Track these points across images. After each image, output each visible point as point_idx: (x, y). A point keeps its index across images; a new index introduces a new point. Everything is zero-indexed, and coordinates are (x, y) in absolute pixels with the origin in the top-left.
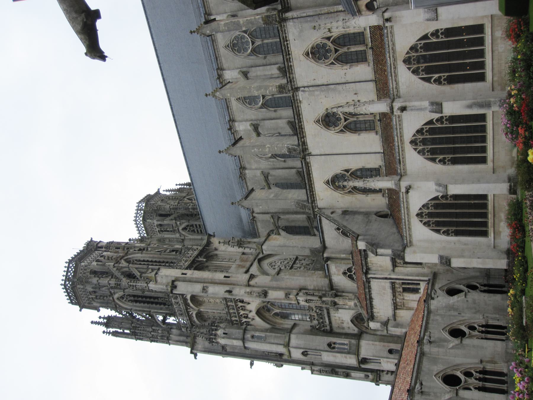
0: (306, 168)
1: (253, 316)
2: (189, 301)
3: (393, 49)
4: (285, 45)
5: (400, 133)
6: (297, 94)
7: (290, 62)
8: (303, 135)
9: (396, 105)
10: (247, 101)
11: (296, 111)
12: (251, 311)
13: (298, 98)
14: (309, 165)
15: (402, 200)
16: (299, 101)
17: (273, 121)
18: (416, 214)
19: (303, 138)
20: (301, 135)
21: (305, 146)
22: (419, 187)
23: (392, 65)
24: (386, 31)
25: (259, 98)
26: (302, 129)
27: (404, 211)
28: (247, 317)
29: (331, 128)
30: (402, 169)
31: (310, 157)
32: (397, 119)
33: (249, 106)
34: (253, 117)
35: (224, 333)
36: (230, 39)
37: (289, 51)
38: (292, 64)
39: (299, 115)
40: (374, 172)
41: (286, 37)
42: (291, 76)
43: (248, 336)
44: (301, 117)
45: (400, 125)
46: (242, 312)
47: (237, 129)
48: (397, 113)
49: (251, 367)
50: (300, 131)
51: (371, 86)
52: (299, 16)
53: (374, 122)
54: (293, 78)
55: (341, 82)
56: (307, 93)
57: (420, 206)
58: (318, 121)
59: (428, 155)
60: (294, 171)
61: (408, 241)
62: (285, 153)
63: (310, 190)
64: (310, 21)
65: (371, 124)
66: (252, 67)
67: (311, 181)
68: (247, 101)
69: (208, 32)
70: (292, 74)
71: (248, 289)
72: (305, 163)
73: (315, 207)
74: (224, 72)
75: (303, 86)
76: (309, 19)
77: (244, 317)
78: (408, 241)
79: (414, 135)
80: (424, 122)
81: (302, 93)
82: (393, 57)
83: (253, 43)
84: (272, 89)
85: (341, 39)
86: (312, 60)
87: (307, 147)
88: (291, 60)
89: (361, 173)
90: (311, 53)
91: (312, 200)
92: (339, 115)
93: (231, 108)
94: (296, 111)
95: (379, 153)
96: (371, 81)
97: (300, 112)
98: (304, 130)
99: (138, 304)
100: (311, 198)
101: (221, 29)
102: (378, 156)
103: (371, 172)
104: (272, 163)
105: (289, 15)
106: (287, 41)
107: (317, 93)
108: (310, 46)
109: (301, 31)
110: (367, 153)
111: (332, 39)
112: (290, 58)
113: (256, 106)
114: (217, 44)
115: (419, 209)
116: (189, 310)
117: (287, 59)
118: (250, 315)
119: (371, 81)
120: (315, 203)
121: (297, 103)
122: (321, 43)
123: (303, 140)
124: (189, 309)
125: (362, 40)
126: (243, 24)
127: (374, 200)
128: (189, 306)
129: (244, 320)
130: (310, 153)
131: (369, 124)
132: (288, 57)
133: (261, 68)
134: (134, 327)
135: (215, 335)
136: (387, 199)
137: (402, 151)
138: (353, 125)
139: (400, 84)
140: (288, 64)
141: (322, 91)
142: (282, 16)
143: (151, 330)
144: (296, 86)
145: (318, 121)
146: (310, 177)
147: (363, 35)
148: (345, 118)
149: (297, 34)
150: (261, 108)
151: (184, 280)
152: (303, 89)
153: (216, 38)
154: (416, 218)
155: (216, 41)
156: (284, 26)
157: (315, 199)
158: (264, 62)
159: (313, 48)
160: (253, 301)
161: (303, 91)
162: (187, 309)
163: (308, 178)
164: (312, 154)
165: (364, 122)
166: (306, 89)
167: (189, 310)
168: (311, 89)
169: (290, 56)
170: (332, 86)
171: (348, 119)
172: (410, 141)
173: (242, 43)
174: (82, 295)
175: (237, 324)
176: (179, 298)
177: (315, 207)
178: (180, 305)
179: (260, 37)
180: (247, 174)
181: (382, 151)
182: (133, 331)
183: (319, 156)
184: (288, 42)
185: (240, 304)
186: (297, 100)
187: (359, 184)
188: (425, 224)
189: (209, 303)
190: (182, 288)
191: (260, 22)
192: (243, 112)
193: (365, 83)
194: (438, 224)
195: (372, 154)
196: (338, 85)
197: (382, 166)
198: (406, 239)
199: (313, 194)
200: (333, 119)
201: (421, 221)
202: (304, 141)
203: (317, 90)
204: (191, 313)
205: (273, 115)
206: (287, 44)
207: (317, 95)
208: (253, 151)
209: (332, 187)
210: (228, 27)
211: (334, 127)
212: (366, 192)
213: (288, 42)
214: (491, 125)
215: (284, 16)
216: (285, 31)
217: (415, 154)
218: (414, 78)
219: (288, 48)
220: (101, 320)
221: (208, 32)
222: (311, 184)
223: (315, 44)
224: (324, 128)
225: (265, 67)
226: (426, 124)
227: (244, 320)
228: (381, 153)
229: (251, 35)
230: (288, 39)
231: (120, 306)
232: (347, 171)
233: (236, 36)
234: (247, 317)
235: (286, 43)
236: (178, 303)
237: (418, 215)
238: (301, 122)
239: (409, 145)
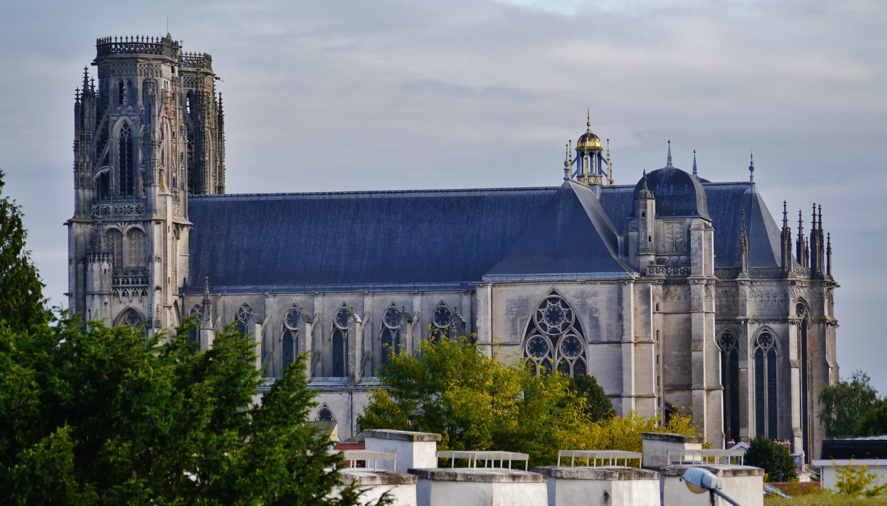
1: (125, 303)
2: (133, 225)
10: (341, 313)
12: (131, 301)
17: (321, 337)
28: (124, 295)
33: (336, 314)
34: (325, 316)
35: (105, 270)
43: (107, 299)
46: (130, 292)
47: (316, 299)
49: (64, 294)
56: (347, 400)
60: (271, 349)
66: (372, 326)
68: (341, 313)
71: (160, 308)
74: (371, 297)
77: (124, 293)
83: (393, 330)
99: (119, 146)
101: (402, 334)
104: (278, 326)
113: (335, 321)
116: (123, 223)
118: (125, 299)
124: (125, 224)
128: (128, 224)
129: (120, 292)
133: (370, 335)
134: (90, 136)
135: (103, 260)
141: (348, 412)
143: (88, 160)
150: (334, 326)
151: (165, 232)
158: (376, 338)
160: (144, 306)
161: (349, 398)
162: (125, 222)
166: (350, 400)
167: (123, 223)
173: (395, 319)
174: (125, 65)
175: (114, 283)
176: (139, 215)
178: (129, 213)
180: (268, 299)
182: (85, 137)
185: (140, 292)
189: (129, 245)
190: (157, 230)
192: (331, 307)
203: (348, 408)
204: (119, 224)
205: (327, 337)
220: (90, 84)
225: (370, 340)
227: (120, 292)
231: (115, 121)
234: (124, 295)
236: (131, 212)
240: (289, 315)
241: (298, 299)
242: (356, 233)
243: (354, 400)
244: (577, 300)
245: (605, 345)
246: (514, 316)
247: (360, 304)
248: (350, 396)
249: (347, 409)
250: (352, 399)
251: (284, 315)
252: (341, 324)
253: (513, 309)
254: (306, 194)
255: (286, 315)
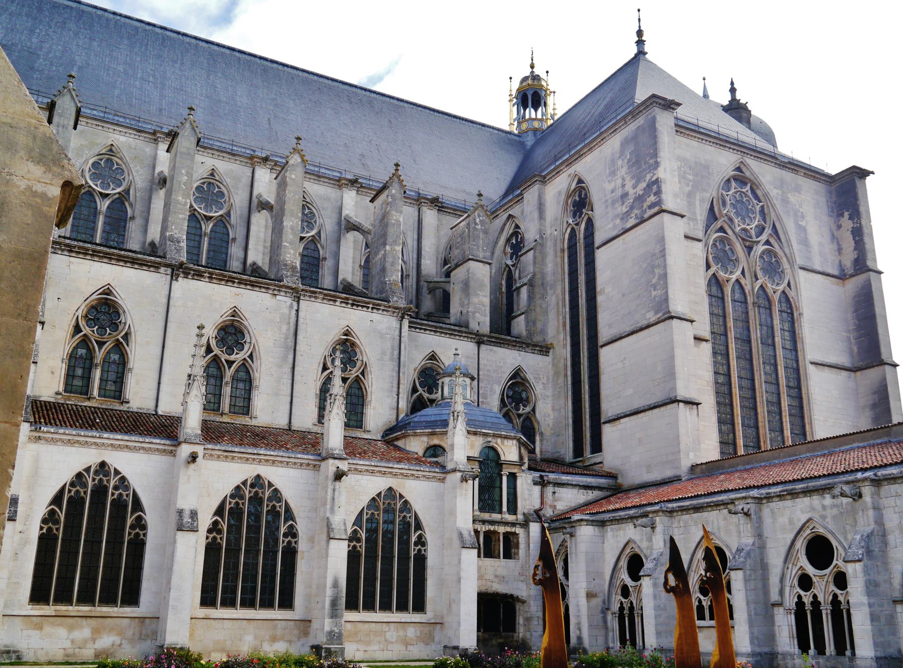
0: (148, 262)
3: (413, 475)
4: (369, 303)
5: (282, 462)
6: (288, 295)
7: (341, 302)
8: (215, 278)
9: (344, 465)
10: (205, 186)
11: (262, 283)
13: (282, 294)
14: (152, 269)
15: (147, 440)
16: (276, 292)
18: (108, 461)
19: (209, 277)
20: (216, 275)
21: (194, 275)
22: (189, 478)
23: (390, 470)
24: (437, 470)
25: (206, 208)
26: (228, 281)
27: (122, 440)
29: (216, 331)
30: (213, 452)
31: (169, 277)
32: (306, 462)
36: (315, 205)
37: (358, 306)
38: (338, 303)
39: (253, 286)
40: (113, 388)
41: (378, 309)
42: (321, 296)
44: (248, 287)
45: (295, 463)
48: (332, 465)
50: (225, 276)
51: (281, 421)
52: (402, 339)
53: (214, 410)
54: (316, 297)
55: (296, 373)
56: (287, 311)
57: (125, 472)
58: (234, 314)
59: (230, 503)
61: (41, 435)
62: (169, 229)
63: (99, 252)
64: (392, 354)
65: (212, 405)
67: (119, 260)
68: (205, 186)
69: (394, 191)
70: (323, 299)
72: (160, 264)
73: (55, 249)
75: (300, 309)
76: (396, 353)
78: (41, 435)
79: (270, 485)
80: (292, 505)
81: (288, 304)
82: (402, 474)
84: (290, 254)
85: (357, 392)
86: (337, 338)
87: (190, 277)
88: (344, 305)
89: (114, 362)
90: (346, 340)
91: (74, 247)
92: (237, 354)
93: (200, 153)
94: (262, 283)
95: (157, 406)
96: (290, 422)
97: (257, 289)
98: (223, 282)
100: (80, 248)
102: (286, 421)
103: (114, 382)
105: (406, 323)
106: (373, 308)
107: (284, 328)
108: (358, 342)
109: (382, 336)
110: (159, 383)
111: (362, 378)
112: (347, 303)
114: (312, 181)
115: (119, 469)
117: (347, 299)
119: (290, 422)
120: (63, 250)
121: (274, 290)
122: (120, 322)
123: (207, 275)
125: (351, 423)
126: (395, 250)
127: (52, 373)
130: (176, 280)
131: (212, 400)
132: (350, 302)
136: (53, 400)
137: (248, 459)
138: (215, 373)
139: (359, 477)
140: (341, 298)
141: (286, 338)
142: (408, 315)
144: (302, 297)
145: (234, 314)
146: (126, 262)
147: (357, 427)
148: (233, 362)
149: (379, 328)
152: (295, 307)
153: (321, 183)
154: (100, 460)
155: (316, 182)
156: (394, 312)
157: (74, 255)
159: (353, 344)
161: (291, 306)
163: (128, 257)
164: (174, 282)
165: (218, 393)
166: (294, 312)
168: (293, 320)
169: (349, 306)
170: (291, 357)
171: (230, 367)
172: (263, 475)
177: (55, 249)
179: (305, 253)
181: (160, 413)
183: (167, 293)
184: (370, 310)
186: (279, 290)
187: (338, 388)
188: (79, 475)
191: (392, 276)
193: (288, 412)
194: (76, 503)
195: (156, 392)
196: (291, 366)
197: (127, 405)
198: (48, 432)
199: (86, 254)
200: (230, 340)
201: (88, 470)
202: (202, 276)
206: (368, 308)
207: (281, 327)
208: (183, 171)
209: (94, 297)
210: (394, 224)
211: (216, 337)
212: (70, 360)
213: (370, 310)
214: (274, 617)
215: (406, 317)
216: (387, 311)
217: (238, 481)
218: (365, 501)
219: (363, 307)
221: (394, 191)
222: (110, 259)
223: (357, 350)
224: (221, 320)
226: (288, 509)
228: (156, 411)
229: (312, 240)
230: (375, 311)
232: (126, 337)
233: (314, 215)
235: (371, 306)
237: (103, 464)
238: (239, 283)
239: (255, 474)
240: (95, 165)
241: (123, 139)
242: (216, 87)
243: (301, 314)
244: (775, 191)
245: (820, 276)
246: (690, 188)
247: (246, 180)
248: (295, 304)
249: (284, 331)
250: (297, 311)
251: (87, 161)
252: (202, 206)
253: (688, 176)
254: (120, 15)
255: (91, 161)
